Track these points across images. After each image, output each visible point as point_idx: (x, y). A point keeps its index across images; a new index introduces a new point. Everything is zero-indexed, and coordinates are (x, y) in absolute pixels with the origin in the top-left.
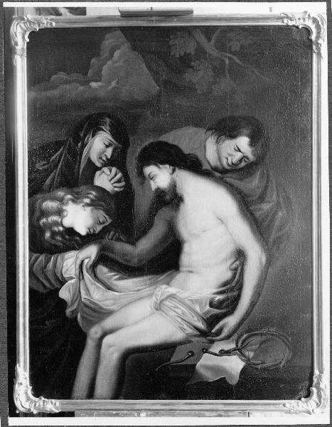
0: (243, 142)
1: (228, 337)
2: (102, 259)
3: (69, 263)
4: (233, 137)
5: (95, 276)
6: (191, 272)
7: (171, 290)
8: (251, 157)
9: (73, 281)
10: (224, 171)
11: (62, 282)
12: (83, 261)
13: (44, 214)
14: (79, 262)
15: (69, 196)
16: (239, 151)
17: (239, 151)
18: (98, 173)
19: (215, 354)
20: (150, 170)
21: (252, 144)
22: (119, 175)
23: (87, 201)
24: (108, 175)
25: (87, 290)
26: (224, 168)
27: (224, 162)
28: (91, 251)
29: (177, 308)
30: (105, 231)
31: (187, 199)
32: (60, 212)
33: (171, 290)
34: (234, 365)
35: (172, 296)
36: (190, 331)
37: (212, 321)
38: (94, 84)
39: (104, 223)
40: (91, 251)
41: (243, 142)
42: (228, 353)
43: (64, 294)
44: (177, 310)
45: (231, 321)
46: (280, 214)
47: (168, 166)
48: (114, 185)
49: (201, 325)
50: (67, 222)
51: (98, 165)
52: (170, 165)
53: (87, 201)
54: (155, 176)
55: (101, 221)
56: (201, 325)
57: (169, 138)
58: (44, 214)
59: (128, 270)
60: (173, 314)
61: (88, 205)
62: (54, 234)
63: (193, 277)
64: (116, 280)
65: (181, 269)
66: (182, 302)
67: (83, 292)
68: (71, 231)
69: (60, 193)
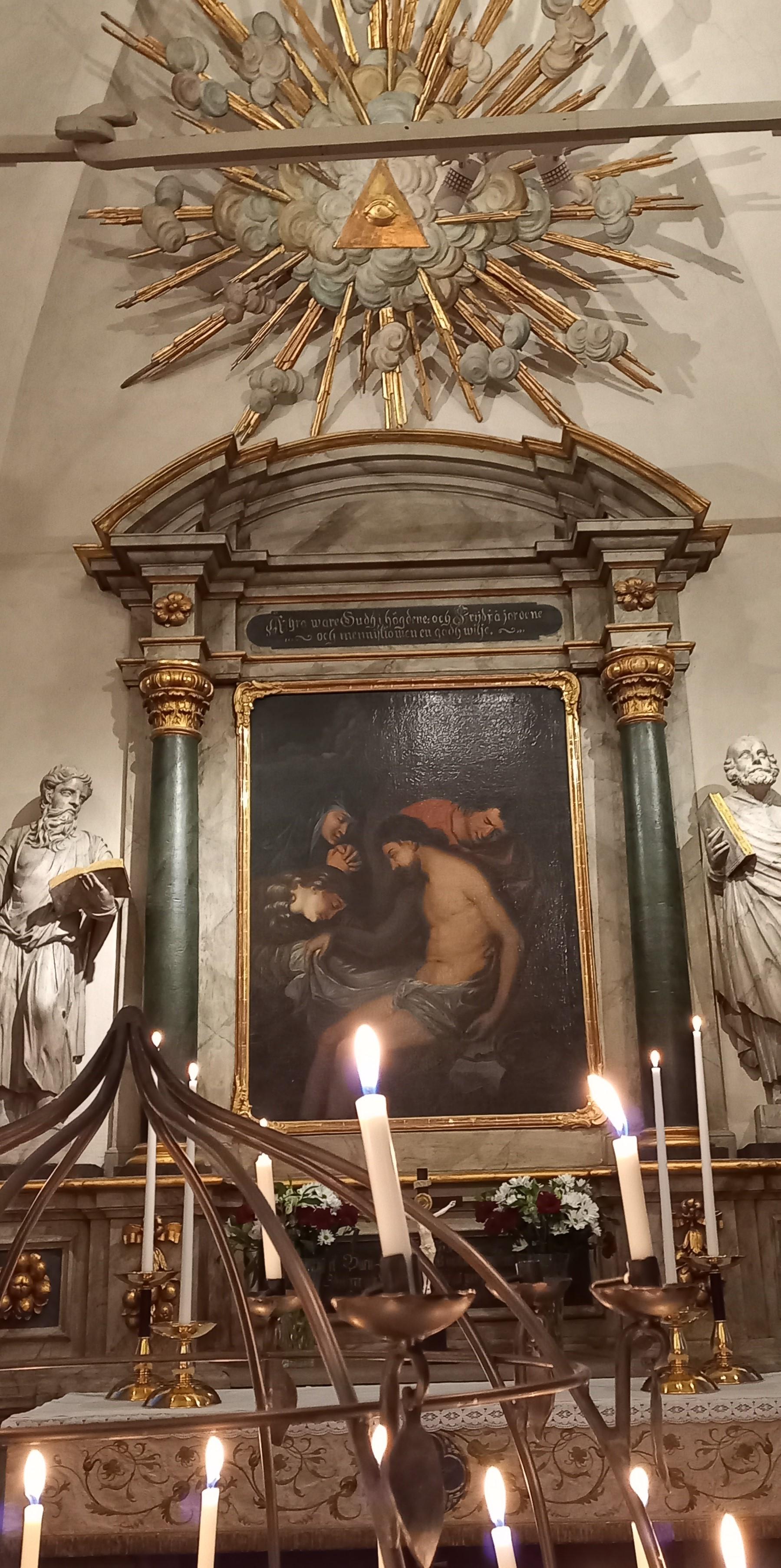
0: (494, 813)
1: (483, 1040)
2: (335, 949)
3: (298, 953)
4: (483, 808)
5: (329, 971)
6: (438, 961)
7: (417, 983)
8: (504, 831)
9: (302, 976)
10: (473, 846)
11: (290, 976)
12: (314, 952)
13: (271, 899)
14: (308, 953)
15: (297, 879)
16: (490, 823)
17: (490, 823)
18: (331, 851)
19: (470, 1060)
20: (391, 846)
21: (502, 816)
22: (355, 854)
23: (318, 883)
24: (342, 854)
25: (318, 986)
26: (473, 842)
27: (474, 835)
28: (324, 941)
29: (426, 1004)
30: (337, 917)
31: (433, 878)
32: (289, 898)
33: (417, 983)
34: (494, 1070)
35: (418, 991)
36: (439, 1031)
37: (464, 1018)
38: (327, 755)
39: (337, 907)
40: (324, 941)
41: (494, 813)
42: (483, 1057)
43: (292, 992)
44: (425, 1007)
45: (487, 1019)
46: (539, 893)
47: (410, 842)
48: (350, 864)
49: (452, 1024)
50: (295, 907)
51: (332, 842)
52: (413, 840)
53: (318, 883)
54: (397, 853)
55: (335, 904)
56: (452, 1024)
57: (410, 811)
58: (271, 899)
59: (366, 962)
60: (418, 1011)
61: (318, 888)
62: (280, 921)
63: (445, 968)
64: (353, 972)
65: (430, 958)
66: (428, 996)
67: (313, 989)
68: (300, 917)
69: (288, 876)
